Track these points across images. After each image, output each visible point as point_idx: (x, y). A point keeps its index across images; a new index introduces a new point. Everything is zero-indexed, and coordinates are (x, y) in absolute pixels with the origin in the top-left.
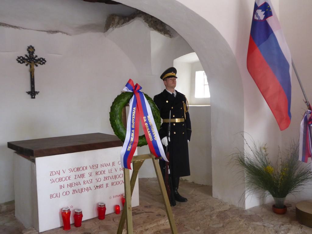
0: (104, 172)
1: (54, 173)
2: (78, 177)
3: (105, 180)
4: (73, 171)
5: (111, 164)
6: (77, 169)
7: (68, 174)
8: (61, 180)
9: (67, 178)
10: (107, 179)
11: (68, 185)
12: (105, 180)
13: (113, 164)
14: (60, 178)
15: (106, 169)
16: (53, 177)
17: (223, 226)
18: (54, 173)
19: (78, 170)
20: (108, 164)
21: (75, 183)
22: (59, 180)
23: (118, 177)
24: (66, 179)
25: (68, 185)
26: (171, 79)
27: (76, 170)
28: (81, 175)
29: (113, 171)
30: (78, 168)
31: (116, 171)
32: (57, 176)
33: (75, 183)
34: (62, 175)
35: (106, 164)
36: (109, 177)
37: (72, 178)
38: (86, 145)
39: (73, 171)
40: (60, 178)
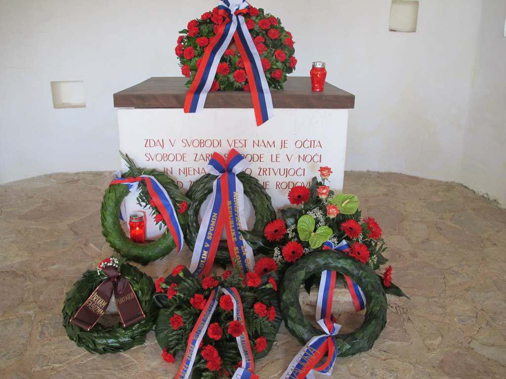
0: (260, 158)
1: (152, 144)
2: (202, 158)
3: (262, 173)
4: (191, 145)
5: (278, 144)
6: (200, 143)
7: (179, 148)
8: (165, 159)
9: (179, 157)
10: (267, 172)
11: (254, 142)
12: (262, 173)
13: (283, 144)
14: (165, 155)
15: (266, 152)
16: (148, 150)
17: (488, 257)
18: (152, 144)
19: (202, 145)
20: (271, 143)
21: (194, 169)
22: (163, 157)
23: (292, 172)
24: (175, 158)
25: (254, 142)
26: (274, 377)
27: (196, 143)
28: (208, 156)
29: (282, 158)
30: (202, 141)
31: (289, 161)
32: (158, 149)
33: (194, 169)
34: (168, 149)
35: (266, 143)
36: (271, 170)
37: (190, 158)
38: (164, 96)
39: (191, 145)
40: (165, 155)
